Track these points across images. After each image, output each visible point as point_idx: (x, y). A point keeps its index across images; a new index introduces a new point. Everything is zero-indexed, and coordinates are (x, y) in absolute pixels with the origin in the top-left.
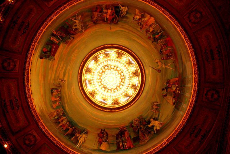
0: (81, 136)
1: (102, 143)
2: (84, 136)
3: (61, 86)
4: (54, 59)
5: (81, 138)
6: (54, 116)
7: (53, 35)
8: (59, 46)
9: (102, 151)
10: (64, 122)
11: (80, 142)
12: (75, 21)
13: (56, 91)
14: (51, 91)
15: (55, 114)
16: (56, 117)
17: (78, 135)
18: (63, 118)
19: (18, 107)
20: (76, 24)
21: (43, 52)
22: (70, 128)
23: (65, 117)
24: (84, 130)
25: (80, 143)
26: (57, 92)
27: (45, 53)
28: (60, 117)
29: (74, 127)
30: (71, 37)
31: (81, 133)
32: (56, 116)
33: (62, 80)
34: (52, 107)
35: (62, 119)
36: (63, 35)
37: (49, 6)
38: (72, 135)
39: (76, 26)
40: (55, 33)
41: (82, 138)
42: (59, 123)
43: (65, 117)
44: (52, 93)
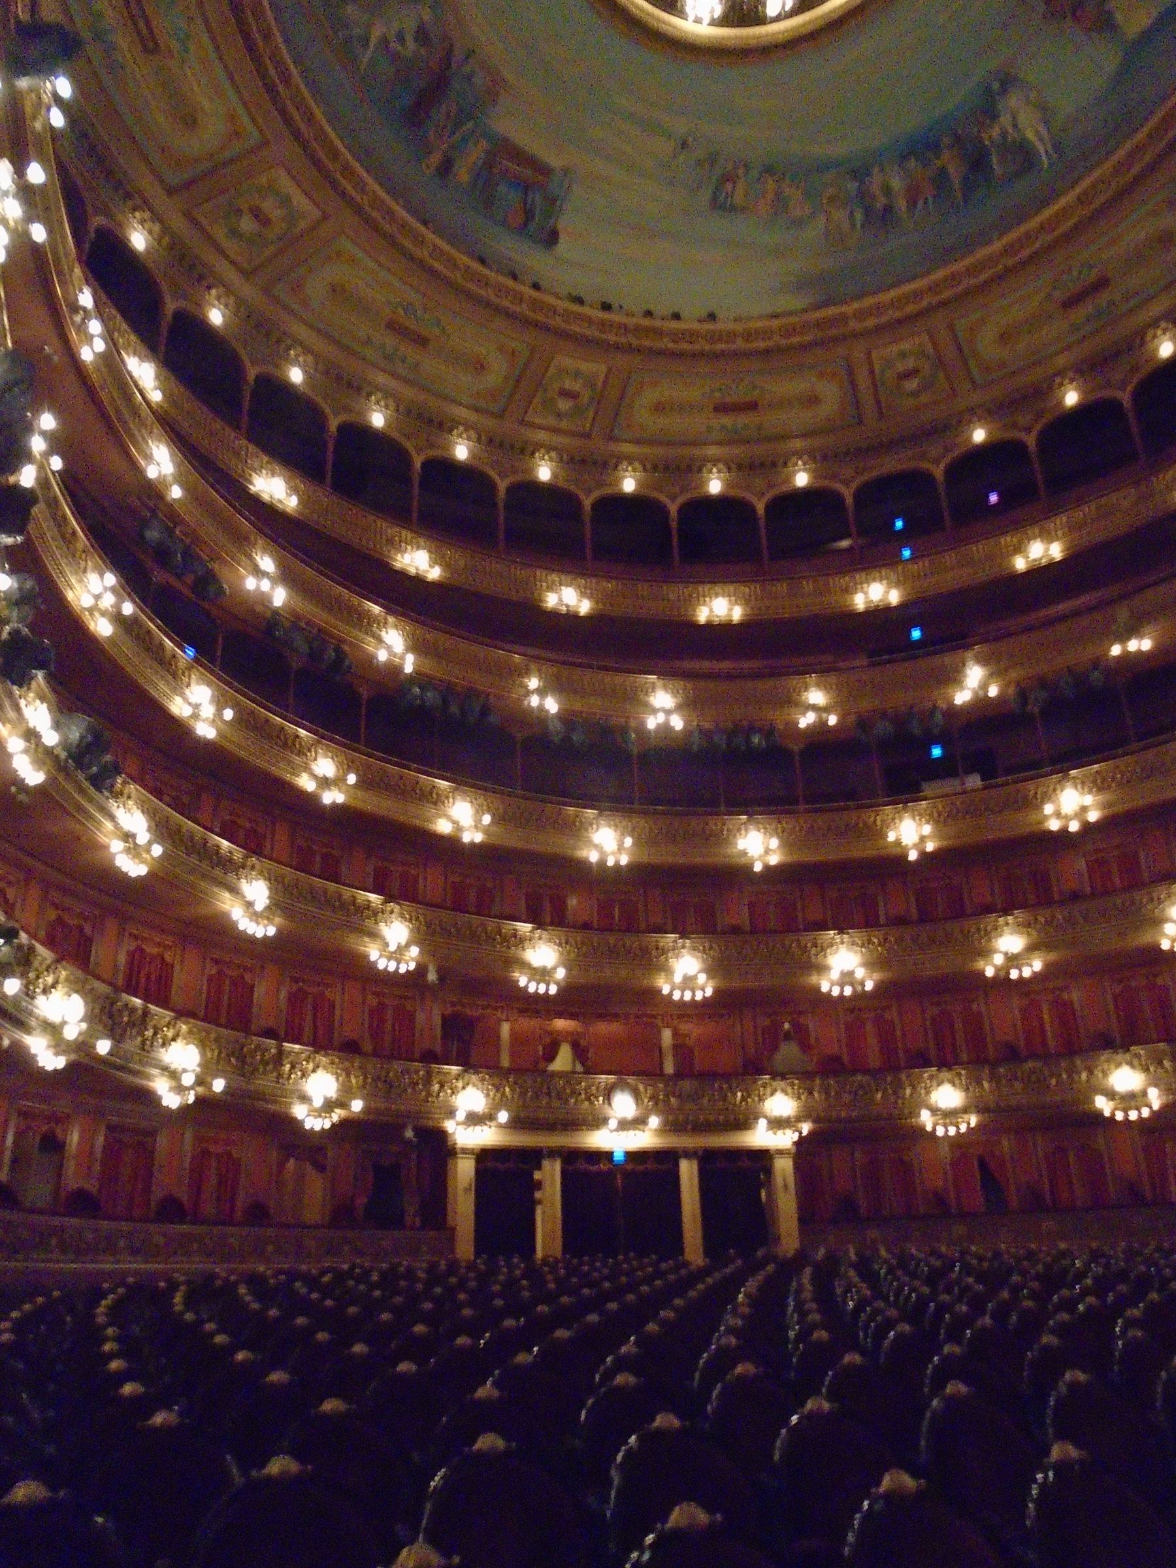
0: (1005, 120)
1: (1109, 13)
2: (1013, 100)
3: (712, 159)
4: (566, 171)
5: (1022, 119)
6: (846, 226)
7: (446, 168)
8: (506, 140)
9: (1146, 37)
10: (896, 184)
11: (1030, 135)
12: (373, 41)
13: (723, 185)
14: (722, 207)
15: (839, 215)
16: (859, 216)
17: (996, 132)
18: (875, 182)
19: (755, 388)
20: (392, 38)
21: (525, 225)
22: (939, 163)
23: (876, 170)
24: (988, 90)
25: (1041, 140)
26: (734, 183)
27: (529, 215)
28: (863, 195)
29: (946, 141)
30: (467, 69)
31: (990, 113)
32: (852, 213)
33: (684, 144)
34: (799, 223)
35: (875, 189)
36: (448, 115)
37: (316, 214)
38: (978, 162)
39: (401, 38)
40: (436, 159)
41: (1020, 117)
42: (888, 209)
43: (876, 170)
44: (733, 209)
